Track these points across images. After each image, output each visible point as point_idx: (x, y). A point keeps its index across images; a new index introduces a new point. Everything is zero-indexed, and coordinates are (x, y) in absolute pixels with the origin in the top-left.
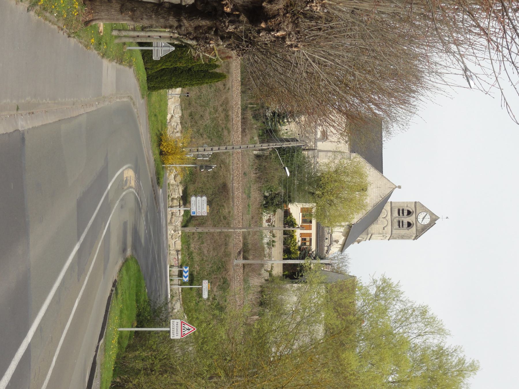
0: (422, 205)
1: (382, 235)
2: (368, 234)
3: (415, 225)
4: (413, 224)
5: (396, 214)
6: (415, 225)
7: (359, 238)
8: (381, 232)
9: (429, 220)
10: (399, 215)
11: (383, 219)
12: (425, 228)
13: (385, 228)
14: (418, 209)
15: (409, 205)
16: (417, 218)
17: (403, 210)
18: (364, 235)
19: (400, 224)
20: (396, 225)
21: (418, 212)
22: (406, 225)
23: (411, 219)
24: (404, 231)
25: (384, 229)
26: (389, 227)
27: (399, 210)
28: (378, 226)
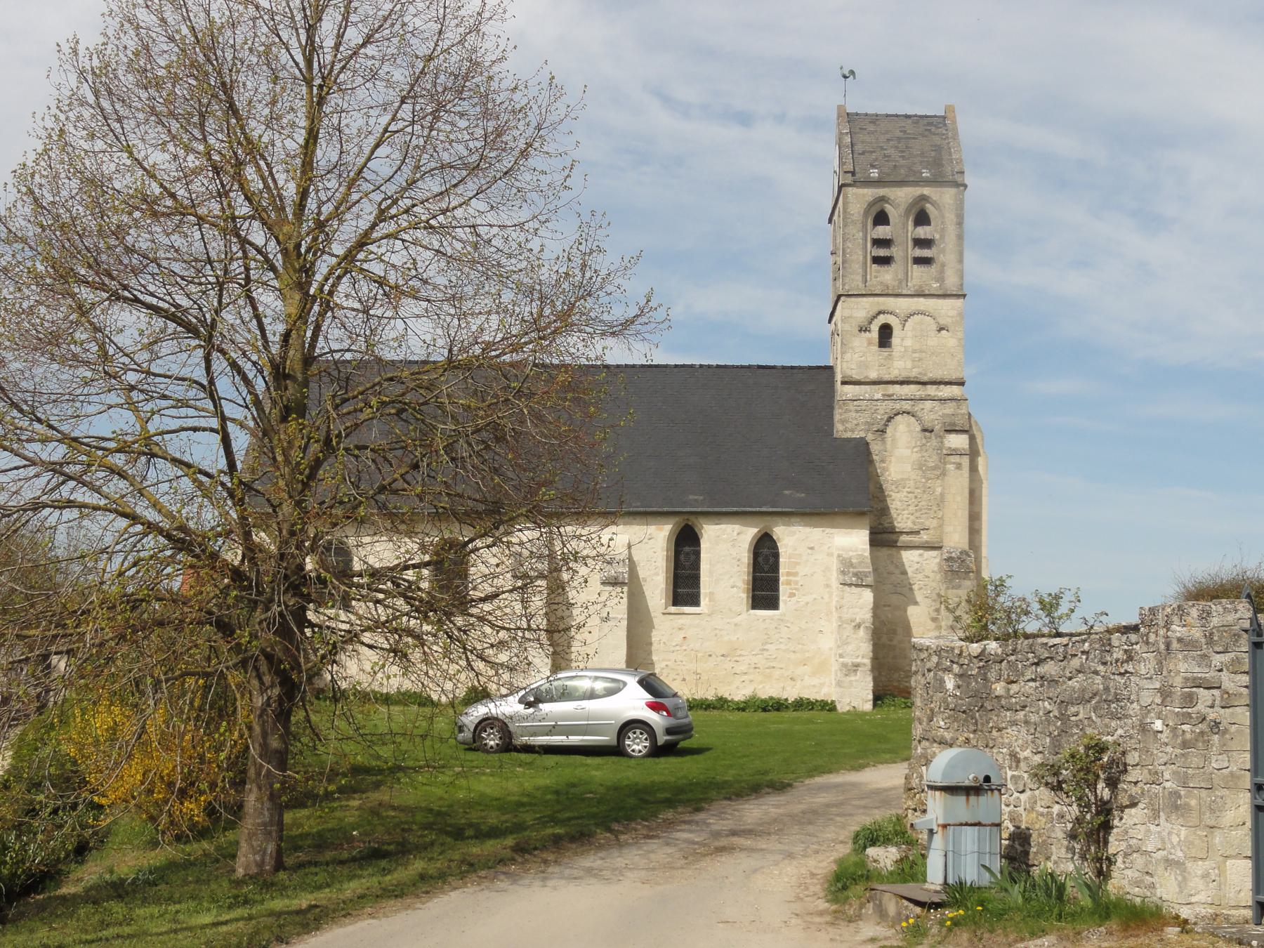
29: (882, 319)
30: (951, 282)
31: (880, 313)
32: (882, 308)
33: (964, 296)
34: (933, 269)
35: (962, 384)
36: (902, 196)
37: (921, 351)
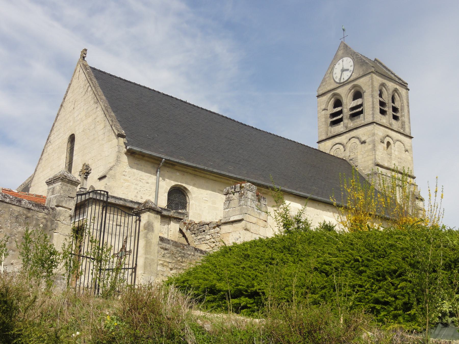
3: (355, 83)
4: (355, 86)
5: (340, 128)
6: (355, 83)
8: (371, 146)
9: (345, 59)
11: (347, 150)
13: (363, 139)
14: (329, 88)
15: (323, 107)
16: (343, 84)
17: (333, 115)
19: (357, 112)
20: (360, 121)
22: (359, 101)
23: (345, 94)
25: (364, 142)
27: (334, 123)
28: (360, 157)
29: (388, 139)
30: (407, 132)
31: (388, 136)
32: (387, 134)
33: (411, 138)
34: (399, 123)
35: (414, 178)
36: (391, 85)
37: (401, 159)
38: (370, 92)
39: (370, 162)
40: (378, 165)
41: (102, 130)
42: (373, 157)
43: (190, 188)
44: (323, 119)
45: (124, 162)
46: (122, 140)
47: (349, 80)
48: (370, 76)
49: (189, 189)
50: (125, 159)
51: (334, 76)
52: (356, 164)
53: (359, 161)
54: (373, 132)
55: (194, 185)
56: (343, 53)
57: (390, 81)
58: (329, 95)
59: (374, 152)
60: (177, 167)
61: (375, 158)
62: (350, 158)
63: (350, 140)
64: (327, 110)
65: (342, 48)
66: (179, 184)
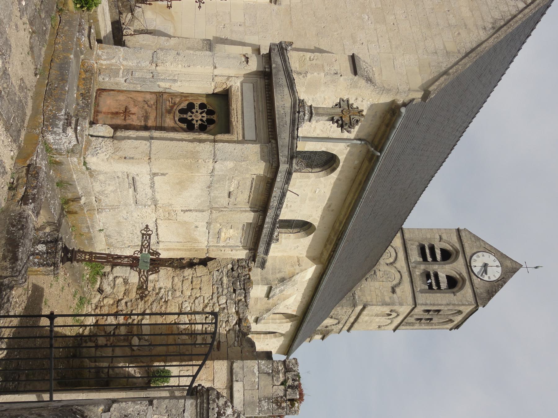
0: (474, 236)
1: (387, 310)
2: (355, 306)
3: (468, 283)
4: (464, 280)
5: (415, 256)
6: (468, 283)
7: (328, 322)
8: (387, 299)
9: (500, 269)
10: (425, 259)
11: (387, 268)
12: (493, 289)
13: (398, 290)
14: (466, 245)
15: (444, 237)
16: (469, 266)
17: (432, 248)
18: (342, 311)
19: (432, 282)
20: (420, 285)
21: (468, 252)
22: (444, 284)
23: (456, 268)
24: (442, 300)
25: (394, 291)
26: (406, 285)
27: (422, 249)
28: (377, 284)
35: (348, 330)
38: (453, 302)
39: (369, 298)
40: (364, 308)
41: (442, 47)
42: (374, 303)
43: (334, 175)
44: (429, 236)
45: (379, 99)
46: (418, 95)
47: (472, 274)
48: (473, 303)
49: (332, 175)
50: (385, 99)
51: (480, 254)
52: (369, 279)
53: (372, 284)
54: (404, 304)
55: (338, 179)
56: (507, 266)
57: (463, 318)
58: (458, 246)
59: (381, 304)
60: (366, 163)
61: (372, 305)
62: (377, 271)
63: (399, 272)
64: (440, 241)
65: (514, 266)
66: (341, 164)
